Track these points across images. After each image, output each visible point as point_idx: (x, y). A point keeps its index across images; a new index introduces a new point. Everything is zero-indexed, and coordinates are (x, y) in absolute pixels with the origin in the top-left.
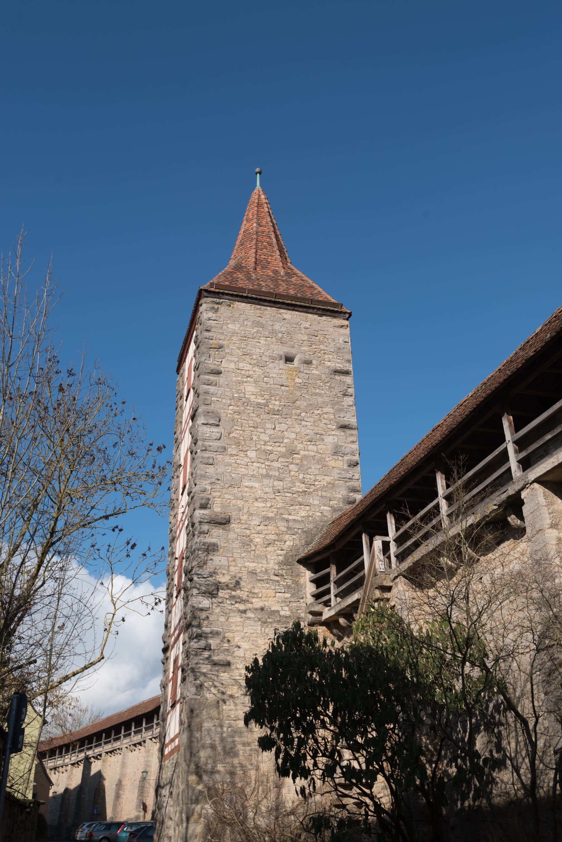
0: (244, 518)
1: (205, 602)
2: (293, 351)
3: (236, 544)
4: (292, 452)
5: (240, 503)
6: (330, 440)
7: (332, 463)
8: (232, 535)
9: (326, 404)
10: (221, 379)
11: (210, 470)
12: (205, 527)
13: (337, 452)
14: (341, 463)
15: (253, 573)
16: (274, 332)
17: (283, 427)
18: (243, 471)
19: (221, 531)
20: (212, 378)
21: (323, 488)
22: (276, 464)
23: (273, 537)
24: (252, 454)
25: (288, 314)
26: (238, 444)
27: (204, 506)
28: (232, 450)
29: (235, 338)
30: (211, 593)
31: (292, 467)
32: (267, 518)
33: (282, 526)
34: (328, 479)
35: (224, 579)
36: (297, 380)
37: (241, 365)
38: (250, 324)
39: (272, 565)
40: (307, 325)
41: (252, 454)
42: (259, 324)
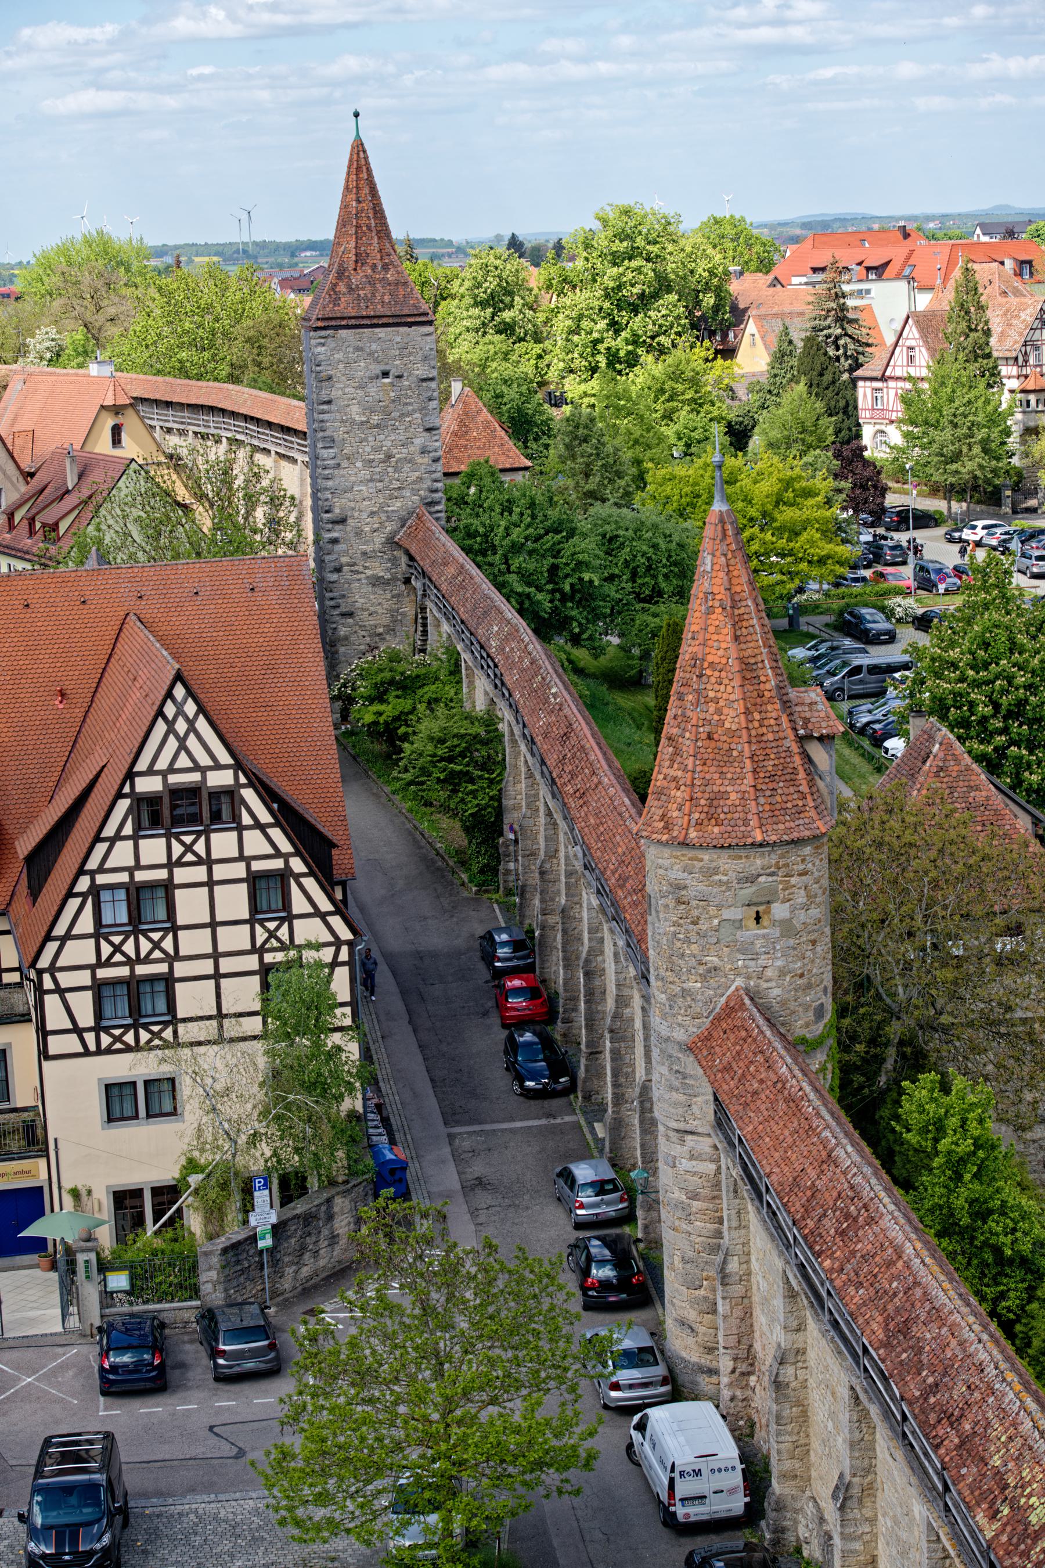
0: (356, 514)
1: (334, 577)
2: (387, 368)
3: (352, 534)
4: (389, 457)
5: (352, 504)
6: (418, 441)
7: (420, 461)
8: (349, 529)
9: (415, 411)
10: (333, 407)
11: (330, 483)
12: (330, 526)
13: (424, 451)
14: (426, 460)
15: (364, 553)
16: (371, 354)
17: (382, 437)
18: (353, 479)
19: (341, 527)
20: (325, 407)
21: (413, 482)
22: (378, 470)
23: (376, 526)
24: (359, 464)
25: (381, 332)
26: (348, 459)
27: (327, 512)
28: (344, 464)
29: (341, 366)
30: (338, 570)
31: (390, 469)
32: (372, 513)
33: (383, 517)
34: (417, 474)
35: (344, 560)
36: (392, 394)
37: (347, 390)
38: (350, 349)
39: (378, 546)
40: (398, 339)
41: (359, 464)
42: (358, 349)
